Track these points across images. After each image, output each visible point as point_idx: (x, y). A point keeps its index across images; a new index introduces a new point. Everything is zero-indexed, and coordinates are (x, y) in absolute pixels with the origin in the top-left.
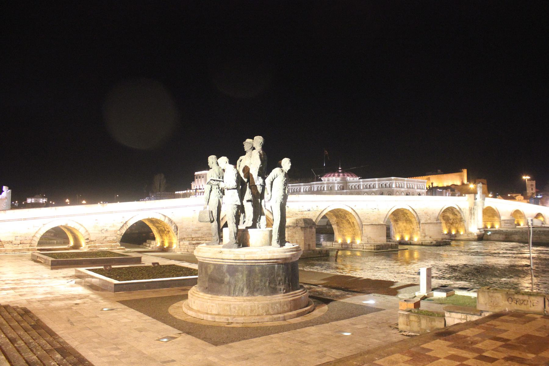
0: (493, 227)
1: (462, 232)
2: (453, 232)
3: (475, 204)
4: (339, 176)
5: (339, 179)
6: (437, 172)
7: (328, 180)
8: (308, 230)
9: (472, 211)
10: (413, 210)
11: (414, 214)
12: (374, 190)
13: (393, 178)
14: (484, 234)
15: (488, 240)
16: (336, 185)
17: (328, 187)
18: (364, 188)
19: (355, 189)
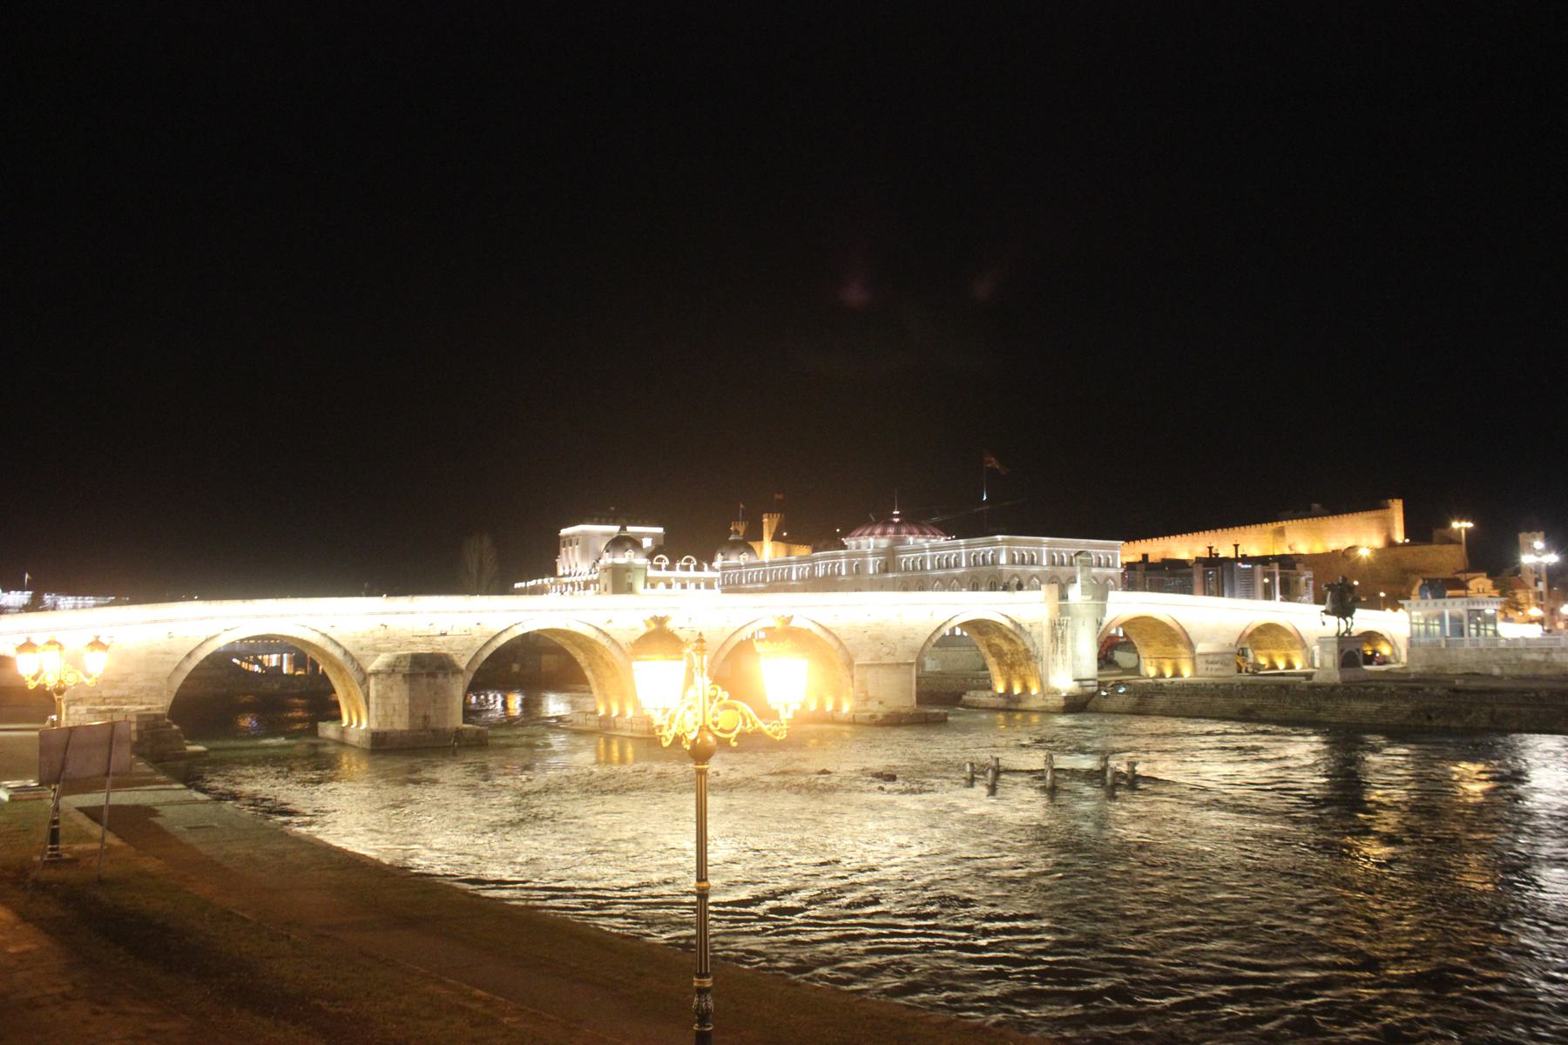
0: (1177, 674)
1: (1034, 691)
2: (1017, 690)
3: (1064, 611)
4: (883, 534)
5: (884, 543)
6: (1309, 509)
7: (858, 547)
8: (424, 680)
9: (1057, 631)
10: (826, 630)
11: (830, 640)
12: (957, 571)
13: (999, 537)
14: (1093, 695)
15: (1097, 711)
16: (871, 559)
17: (849, 565)
18: (933, 568)
19: (914, 569)
